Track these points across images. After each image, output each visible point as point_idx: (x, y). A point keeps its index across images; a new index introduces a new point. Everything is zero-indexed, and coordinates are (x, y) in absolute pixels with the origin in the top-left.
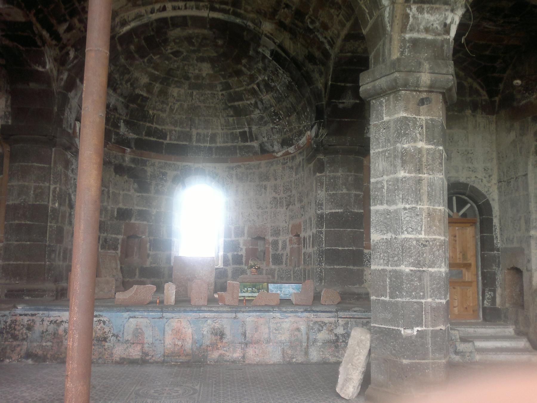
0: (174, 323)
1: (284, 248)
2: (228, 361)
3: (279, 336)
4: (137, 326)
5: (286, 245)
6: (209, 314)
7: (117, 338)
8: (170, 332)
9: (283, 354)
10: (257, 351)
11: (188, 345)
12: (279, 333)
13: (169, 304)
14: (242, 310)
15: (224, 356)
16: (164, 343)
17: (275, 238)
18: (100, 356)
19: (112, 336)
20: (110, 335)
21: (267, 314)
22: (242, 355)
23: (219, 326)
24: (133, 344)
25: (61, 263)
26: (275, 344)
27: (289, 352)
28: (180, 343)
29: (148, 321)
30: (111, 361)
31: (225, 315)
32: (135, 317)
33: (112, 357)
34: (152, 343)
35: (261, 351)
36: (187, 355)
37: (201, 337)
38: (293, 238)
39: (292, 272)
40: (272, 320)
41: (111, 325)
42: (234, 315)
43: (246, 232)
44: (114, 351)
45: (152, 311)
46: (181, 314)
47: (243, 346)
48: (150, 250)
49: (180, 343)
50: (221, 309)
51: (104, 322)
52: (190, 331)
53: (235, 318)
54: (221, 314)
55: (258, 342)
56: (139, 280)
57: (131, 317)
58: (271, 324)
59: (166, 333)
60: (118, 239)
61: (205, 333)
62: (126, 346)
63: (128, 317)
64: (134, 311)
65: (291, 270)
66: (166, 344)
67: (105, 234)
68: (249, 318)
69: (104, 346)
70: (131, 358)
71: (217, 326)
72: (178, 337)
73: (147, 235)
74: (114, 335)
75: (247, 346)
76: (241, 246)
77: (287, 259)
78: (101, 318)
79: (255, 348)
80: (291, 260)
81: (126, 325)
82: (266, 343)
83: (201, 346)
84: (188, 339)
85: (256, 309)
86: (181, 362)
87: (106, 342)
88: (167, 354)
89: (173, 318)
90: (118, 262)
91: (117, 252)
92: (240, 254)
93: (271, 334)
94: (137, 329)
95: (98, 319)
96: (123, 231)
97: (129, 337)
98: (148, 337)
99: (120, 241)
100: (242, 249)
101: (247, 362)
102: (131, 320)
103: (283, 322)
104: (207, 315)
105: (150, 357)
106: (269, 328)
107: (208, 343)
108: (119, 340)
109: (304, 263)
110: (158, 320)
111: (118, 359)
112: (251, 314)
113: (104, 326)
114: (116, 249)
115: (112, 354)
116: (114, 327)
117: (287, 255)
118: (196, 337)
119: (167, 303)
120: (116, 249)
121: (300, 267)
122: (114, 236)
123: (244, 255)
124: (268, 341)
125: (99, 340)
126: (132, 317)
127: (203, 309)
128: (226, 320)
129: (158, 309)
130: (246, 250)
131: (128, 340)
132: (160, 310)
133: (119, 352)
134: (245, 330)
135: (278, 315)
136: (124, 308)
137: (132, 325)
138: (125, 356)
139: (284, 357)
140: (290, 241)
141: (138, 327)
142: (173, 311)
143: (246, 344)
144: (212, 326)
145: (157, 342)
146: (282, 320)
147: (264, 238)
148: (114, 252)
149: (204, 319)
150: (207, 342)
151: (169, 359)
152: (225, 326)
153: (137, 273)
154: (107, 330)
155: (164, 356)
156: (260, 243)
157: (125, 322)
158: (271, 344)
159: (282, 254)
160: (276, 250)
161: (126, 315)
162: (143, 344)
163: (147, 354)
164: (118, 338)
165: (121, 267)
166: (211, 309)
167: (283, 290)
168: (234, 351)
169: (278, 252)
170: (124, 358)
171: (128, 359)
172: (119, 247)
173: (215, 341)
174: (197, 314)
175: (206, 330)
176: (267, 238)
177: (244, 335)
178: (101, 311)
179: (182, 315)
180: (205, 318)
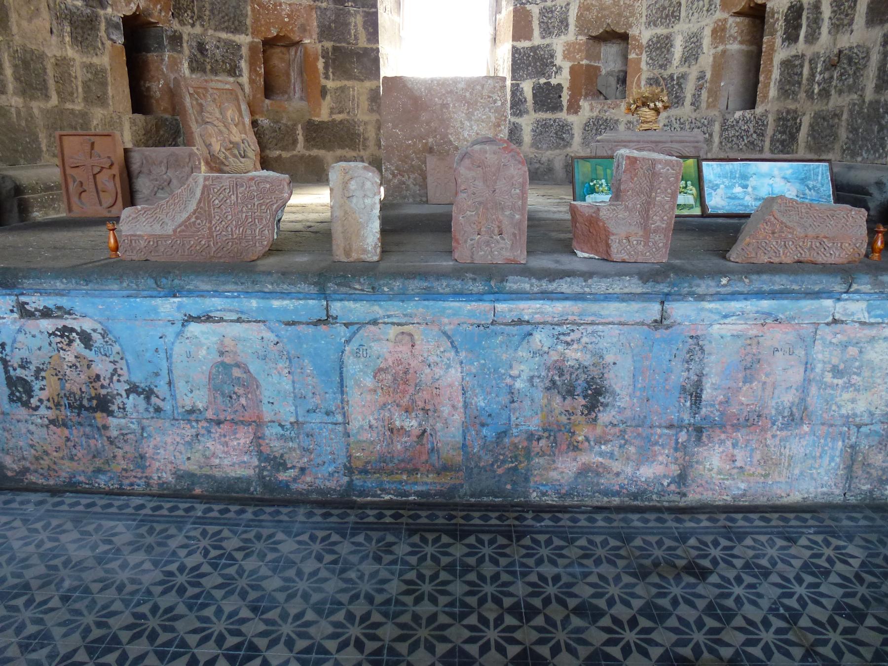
0: (384, 345)
1: (692, 54)
2: (617, 494)
3: (846, 396)
4: (221, 354)
5: (700, 46)
6: (537, 304)
7: (148, 399)
8: (369, 382)
9: (849, 468)
10: (740, 456)
11: (450, 429)
12: (849, 385)
13: (354, 256)
14: (700, 290)
15: (598, 474)
16: (346, 423)
17: (661, 31)
18: (98, 463)
19: (128, 392)
20: (122, 388)
21: (807, 305)
22: (675, 470)
23: (587, 359)
24: (219, 423)
25: (16, 101)
26: (821, 430)
27: (878, 459)
28: (412, 424)
29: (270, 336)
30: (142, 482)
31: (613, 310)
32: (209, 319)
33: (144, 468)
34: (296, 423)
35: (758, 456)
36: (446, 468)
37: (504, 399)
38: (731, 20)
39: (717, 127)
40: (825, 332)
41: (117, 348)
42: (654, 310)
43: (572, 20)
44: (148, 448)
45: (283, 295)
46: (410, 307)
47: (683, 437)
48: (327, 78)
49: (412, 424)
50: (600, 286)
51: (86, 339)
52: (454, 375)
53: (659, 323)
54: (594, 307)
55: (752, 422)
56: (307, 153)
57: (191, 319)
58: (818, 346)
59: (349, 382)
60: (239, 47)
61: (519, 384)
62: (189, 432)
63: (179, 316)
64: (202, 294)
65: (711, 122)
66: (354, 426)
67: (198, 30)
68: (720, 320)
69: (106, 427)
70: (218, 474)
71: (574, 355)
72: (405, 401)
73: (315, 36)
74: (133, 389)
75: (699, 439)
76: (559, 60)
77: (700, 88)
78: (69, 323)
79: (734, 446)
80: (714, 94)
81: (178, 350)
82: (785, 427)
83: (502, 435)
84: (446, 410)
85: (766, 288)
86: (419, 494)
87: (111, 413)
88: (359, 464)
89: (375, 322)
90: (244, 107)
91: (240, 80)
92: (554, 81)
93: (813, 390)
94: (222, 364)
95: (60, 323)
96: (249, 21)
97: (200, 399)
98: (278, 394)
99: (244, 51)
100: (560, 69)
101: (694, 497)
102: (194, 328)
103: (872, 340)
104: (528, 309)
105: (292, 473)
106: (808, 366)
107: (534, 425)
108: (158, 410)
109: (785, 92)
110: (311, 329)
111: (168, 477)
112: (735, 305)
113: (89, 354)
114: (233, 71)
115: (142, 457)
116: (130, 357)
117: (701, 77)
118: (480, 402)
119: (348, 253)
120: (233, 71)
121: (759, 110)
122: (224, 35)
123: (566, 85)
124: (795, 418)
125: (81, 407)
126: (197, 319)
127: (513, 284)
128: (615, 330)
129: (303, 287)
130: (572, 70)
131: (191, 412)
132: (313, 290)
133: (167, 453)
134: (700, 376)
135: (855, 308)
136: (151, 282)
137: (203, 352)
138: (191, 467)
139: (849, 477)
140: (719, 33)
141: (227, 360)
142: (374, 294)
143: (699, 430)
144: (554, 356)
145: (317, 418)
146: (873, 332)
147: (624, 38)
148: (232, 79)
149: (514, 330)
150: (528, 419)
151: (370, 482)
152: (609, 358)
153: (300, 138)
154: (102, 367)
155: (349, 470)
156: (610, 51)
157: (170, 338)
158: (806, 428)
159: (683, 76)
160: (663, 66)
161: (168, 307)
162: (258, 423)
163: (280, 464)
164: (154, 400)
165: (254, 123)
166: (552, 286)
167: (752, 182)
168: (645, 456)
169: (670, 71)
170: (192, 475)
171: (208, 477)
172: (244, 65)
173: (564, 419)
174: (485, 306)
175: (523, 368)
176: (633, 32)
177: (695, 395)
178: (60, 293)
179: (416, 308)
180: (520, 322)
